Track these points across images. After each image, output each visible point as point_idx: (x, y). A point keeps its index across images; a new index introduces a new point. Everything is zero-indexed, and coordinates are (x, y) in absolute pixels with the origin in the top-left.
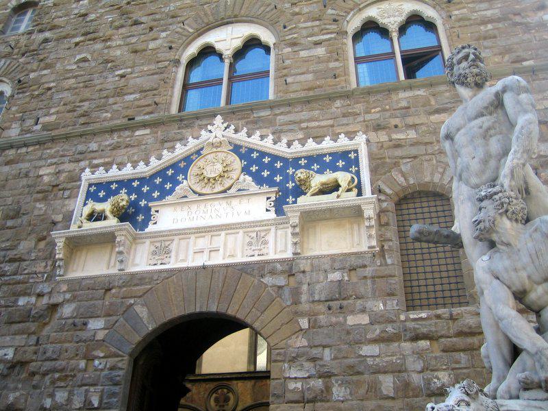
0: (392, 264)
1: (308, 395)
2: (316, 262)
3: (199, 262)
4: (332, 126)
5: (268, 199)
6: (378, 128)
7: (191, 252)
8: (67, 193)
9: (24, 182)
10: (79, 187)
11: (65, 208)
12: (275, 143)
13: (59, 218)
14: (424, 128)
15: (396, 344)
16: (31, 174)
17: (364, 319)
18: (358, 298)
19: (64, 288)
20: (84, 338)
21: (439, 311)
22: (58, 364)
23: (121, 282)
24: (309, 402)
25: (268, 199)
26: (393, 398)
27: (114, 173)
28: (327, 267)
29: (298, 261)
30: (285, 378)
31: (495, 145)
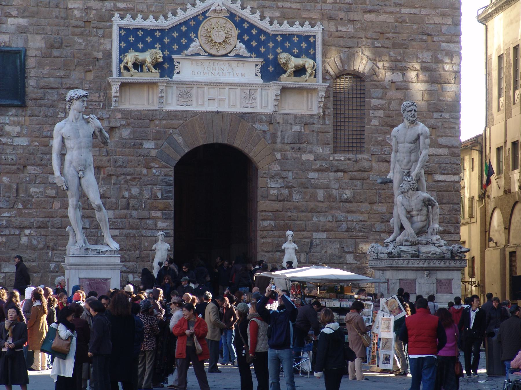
0: (329, 125)
1: (280, 198)
2: (285, 117)
3: (213, 107)
4: (299, 9)
5: (256, 65)
6: (330, 19)
7: (206, 99)
8: (101, 32)
9: (56, 12)
10: (111, 27)
11: (102, 46)
12: (262, 17)
13: (100, 55)
14: (359, 25)
15: (326, 173)
16: (61, 6)
17: (311, 157)
18: (308, 143)
19: (119, 116)
20: (143, 154)
21: (351, 156)
22: (129, 170)
23: (161, 116)
24: (280, 201)
25: (256, 65)
26: (323, 202)
27: (139, 22)
28: (292, 121)
29: (275, 115)
30: (268, 187)
31: (413, 158)
